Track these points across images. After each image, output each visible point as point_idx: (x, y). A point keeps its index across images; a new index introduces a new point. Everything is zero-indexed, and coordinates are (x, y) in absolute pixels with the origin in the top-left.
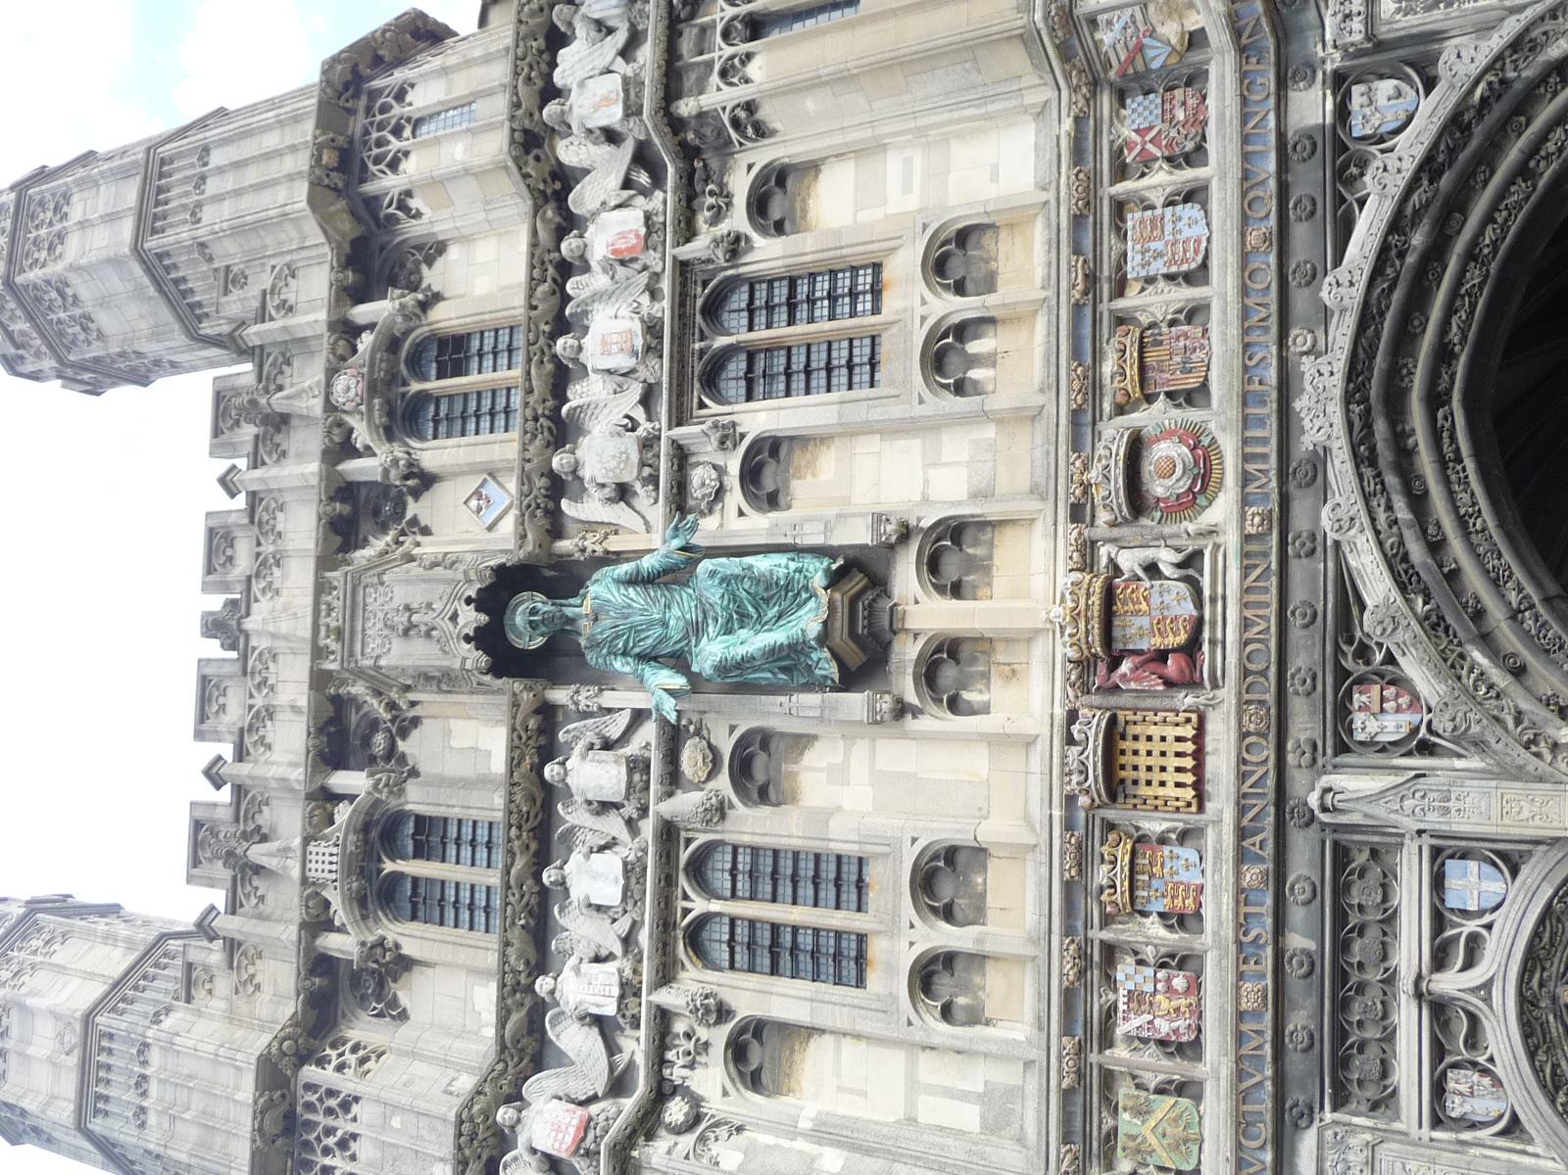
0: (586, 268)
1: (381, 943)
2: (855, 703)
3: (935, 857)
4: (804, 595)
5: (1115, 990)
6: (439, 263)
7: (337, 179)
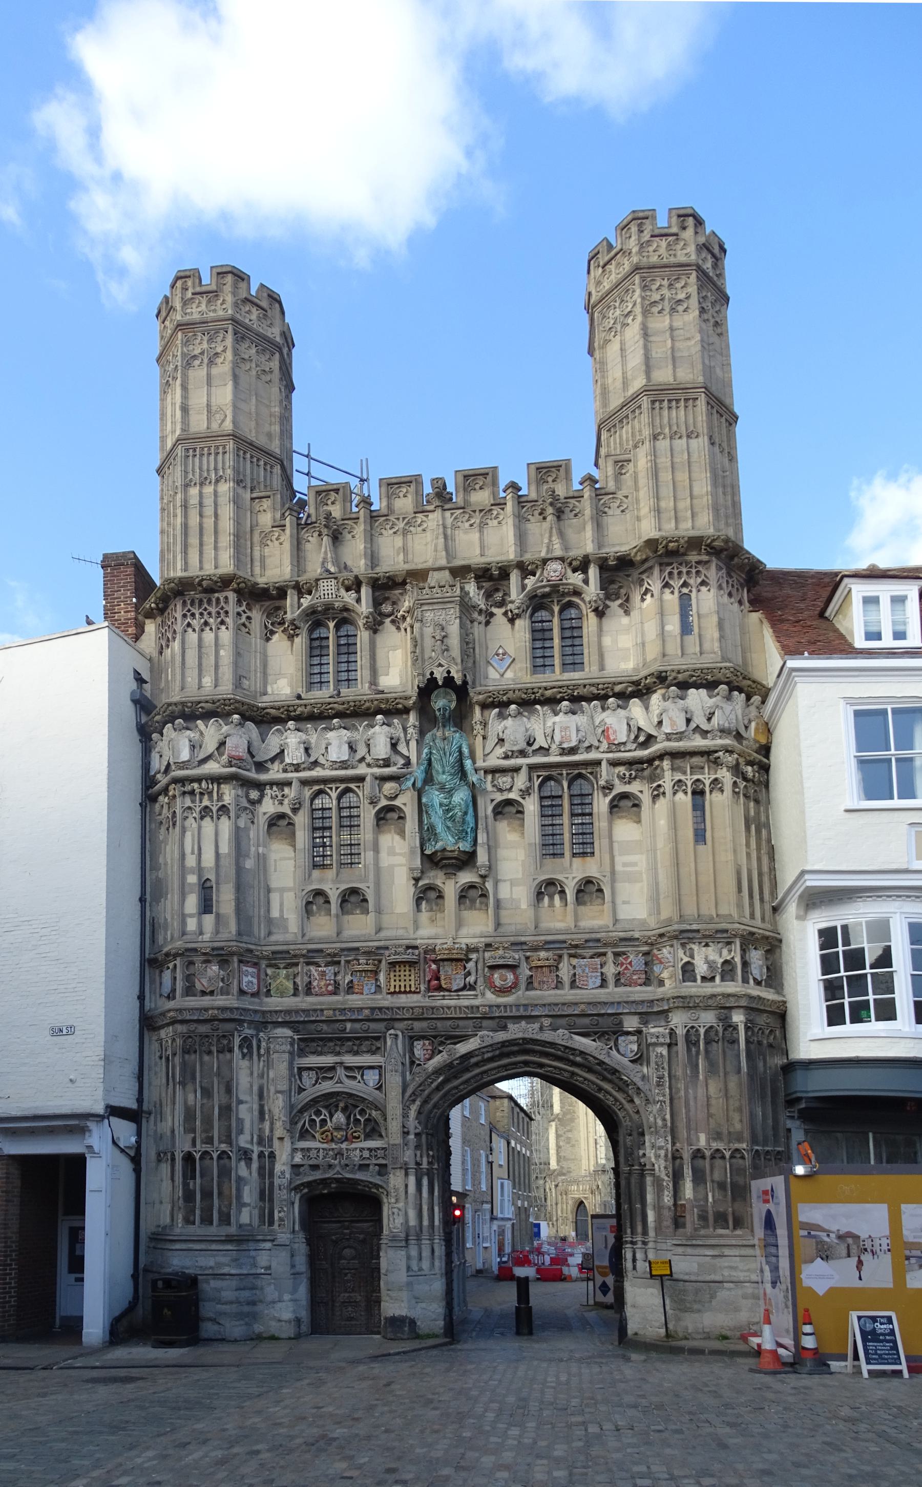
0: (604, 709)
3: (364, 895)
6: (621, 611)
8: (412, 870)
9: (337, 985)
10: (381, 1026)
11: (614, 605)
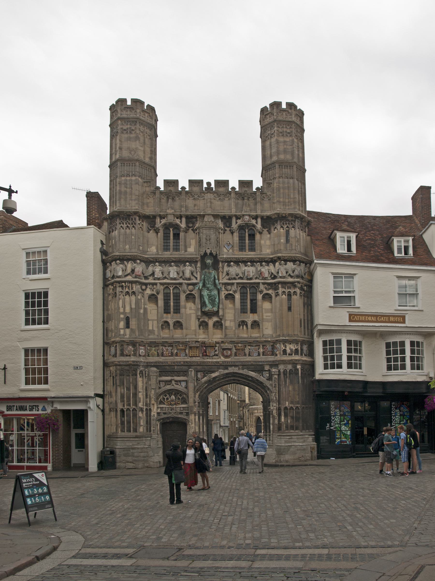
1: (159, 230)
2: (200, 313)
6: (267, 233)
8: (197, 316)
10: (186, 368)
11: (265, 230)
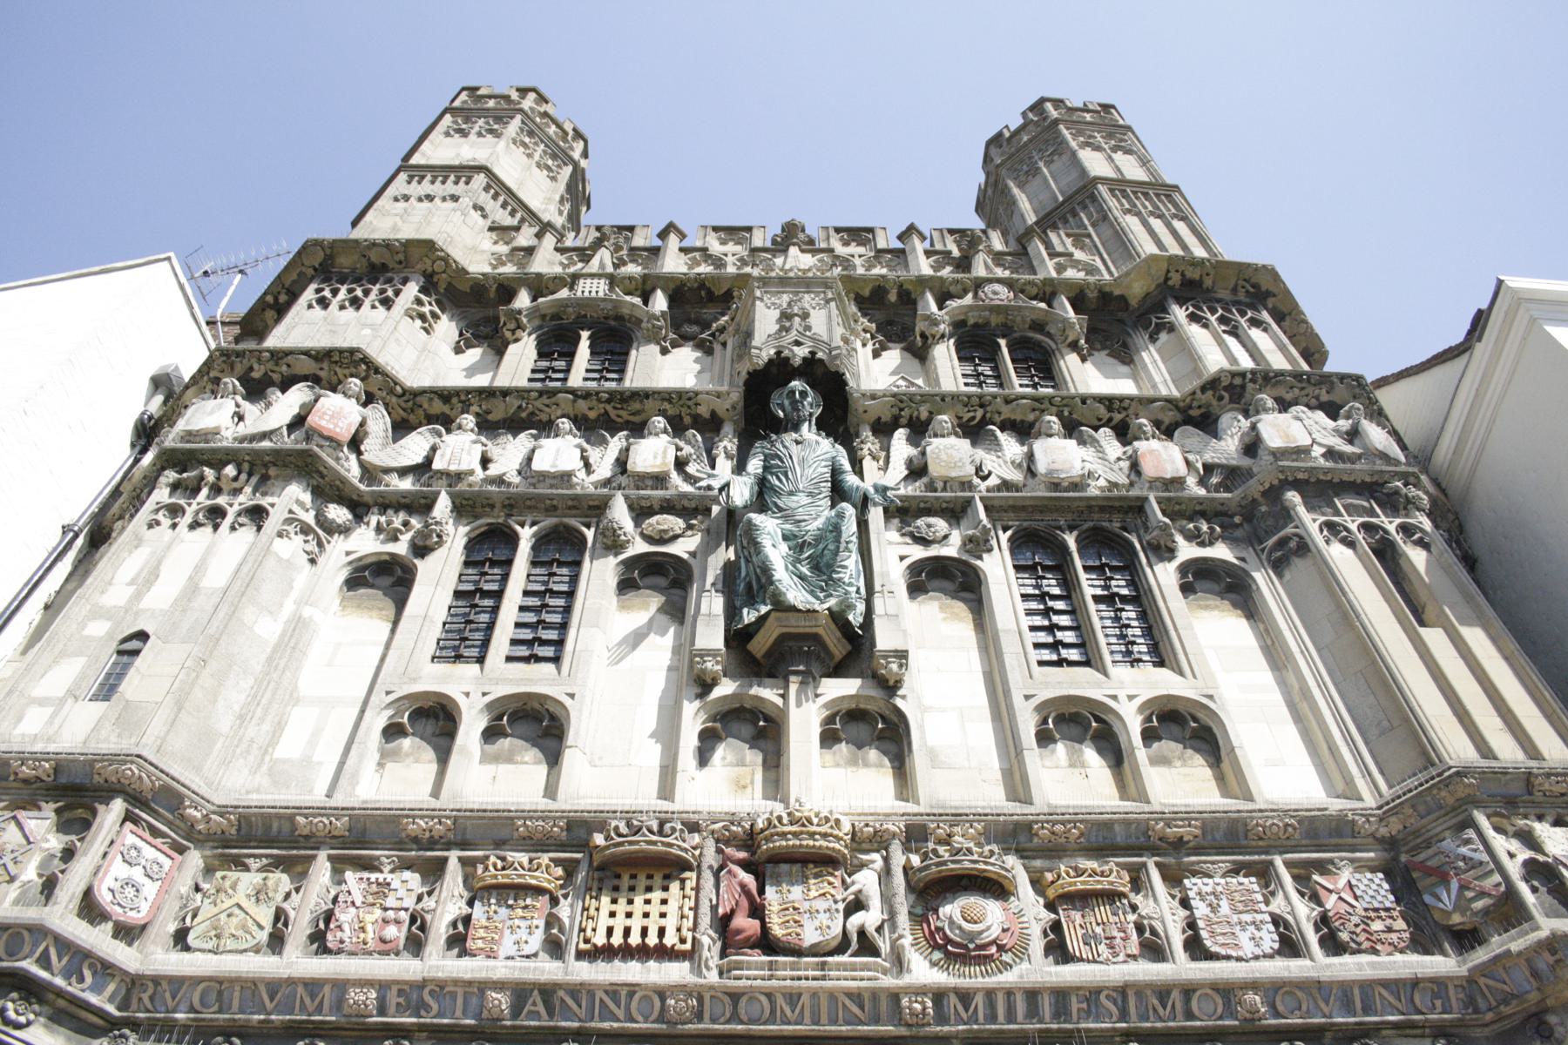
1: (520, 327)
4: (822, 595)
5: (392, 871)
7: (1175, 279)
9: (418, 926)
